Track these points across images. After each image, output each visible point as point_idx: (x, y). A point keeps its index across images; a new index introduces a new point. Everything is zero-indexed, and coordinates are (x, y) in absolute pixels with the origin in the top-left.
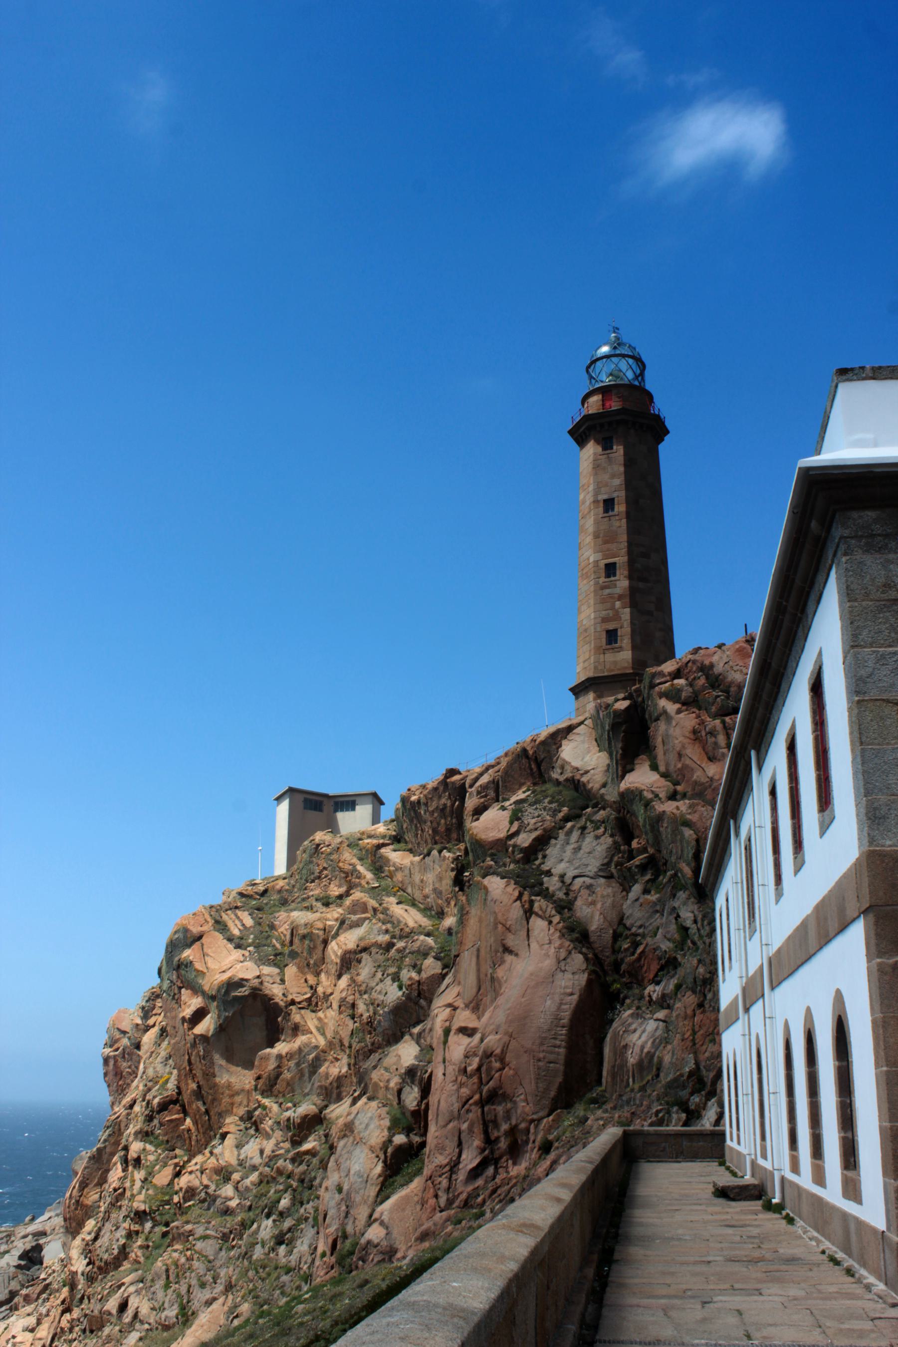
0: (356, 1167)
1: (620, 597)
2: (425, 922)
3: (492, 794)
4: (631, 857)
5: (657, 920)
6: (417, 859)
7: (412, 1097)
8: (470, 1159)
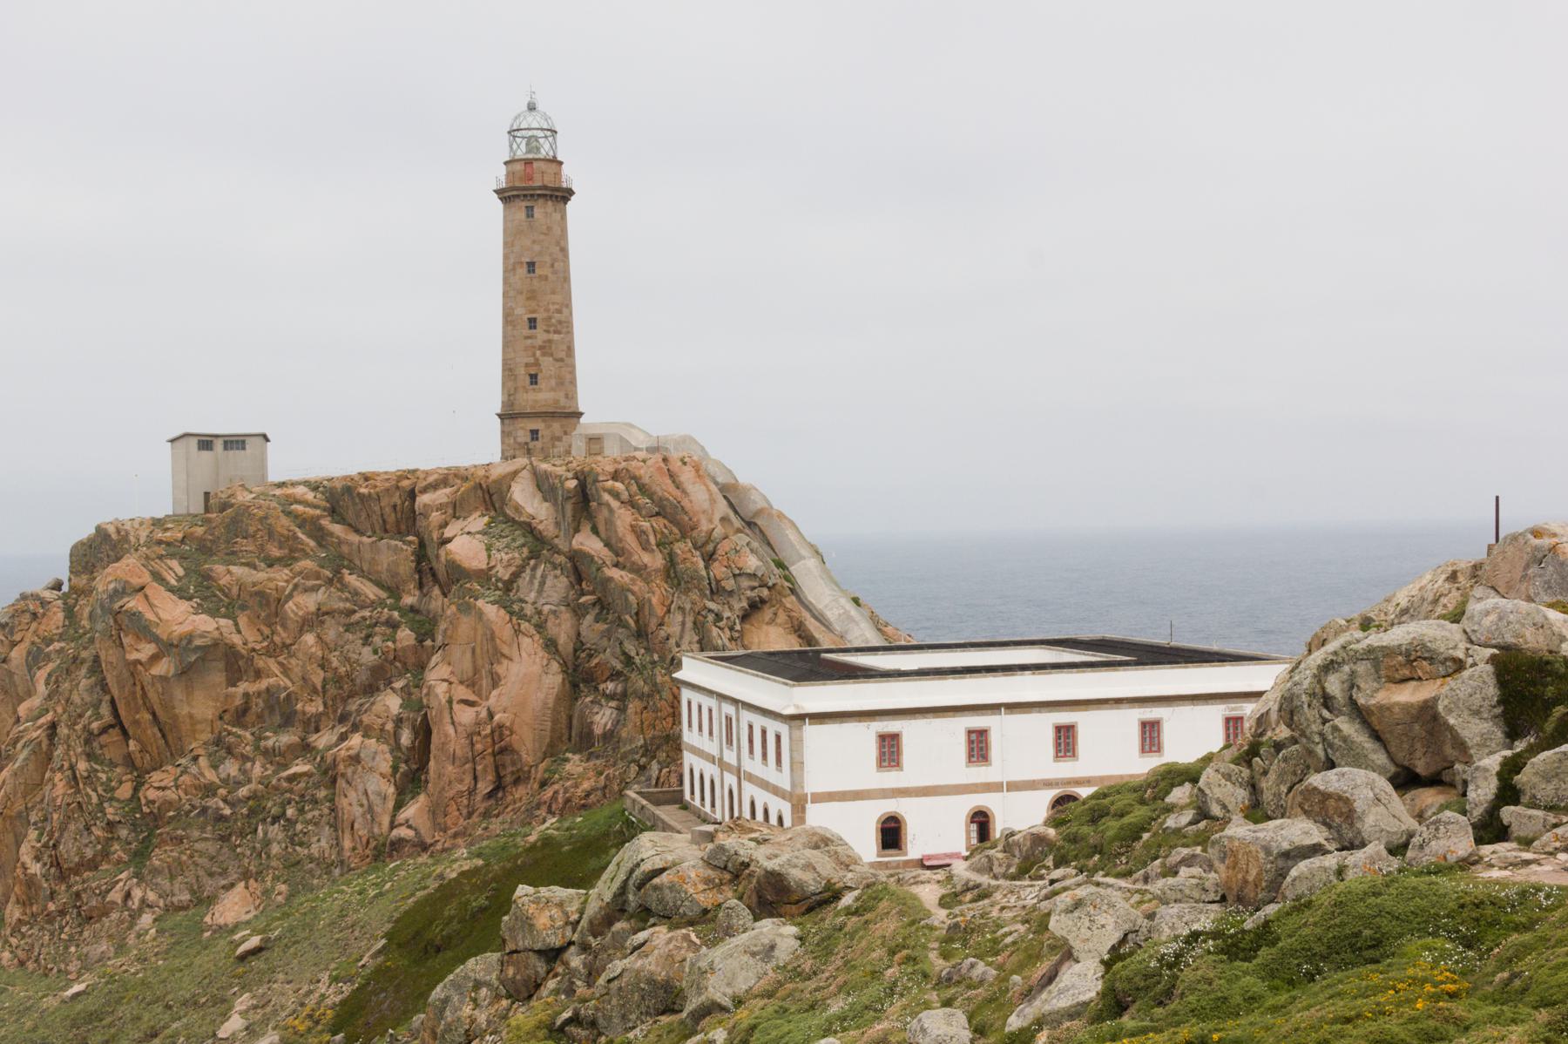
0: (371, 788)
1: (541, 348)
2: (384, 595)
3: (450, 511)
4: (583, 594)
5: (605, 642)
6: (365, 539)
7: (406, 738)
8: (484, 787)
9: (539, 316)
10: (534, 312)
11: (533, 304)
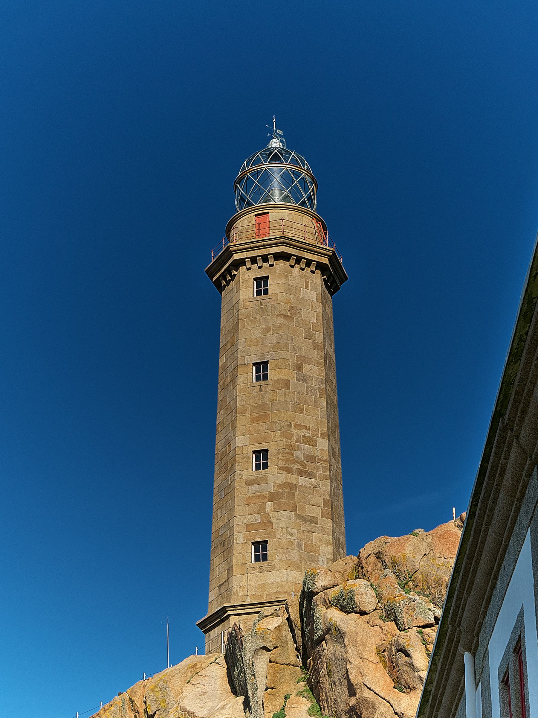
1: (273, 497)
9: (272, 447)
10: (265, 440)
11: (263, 427)
